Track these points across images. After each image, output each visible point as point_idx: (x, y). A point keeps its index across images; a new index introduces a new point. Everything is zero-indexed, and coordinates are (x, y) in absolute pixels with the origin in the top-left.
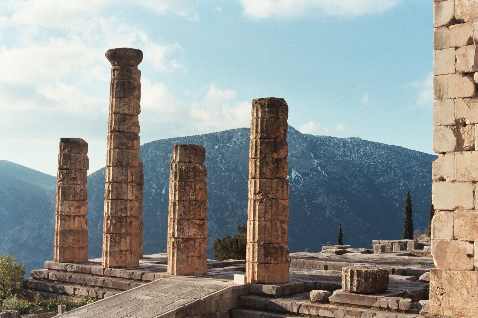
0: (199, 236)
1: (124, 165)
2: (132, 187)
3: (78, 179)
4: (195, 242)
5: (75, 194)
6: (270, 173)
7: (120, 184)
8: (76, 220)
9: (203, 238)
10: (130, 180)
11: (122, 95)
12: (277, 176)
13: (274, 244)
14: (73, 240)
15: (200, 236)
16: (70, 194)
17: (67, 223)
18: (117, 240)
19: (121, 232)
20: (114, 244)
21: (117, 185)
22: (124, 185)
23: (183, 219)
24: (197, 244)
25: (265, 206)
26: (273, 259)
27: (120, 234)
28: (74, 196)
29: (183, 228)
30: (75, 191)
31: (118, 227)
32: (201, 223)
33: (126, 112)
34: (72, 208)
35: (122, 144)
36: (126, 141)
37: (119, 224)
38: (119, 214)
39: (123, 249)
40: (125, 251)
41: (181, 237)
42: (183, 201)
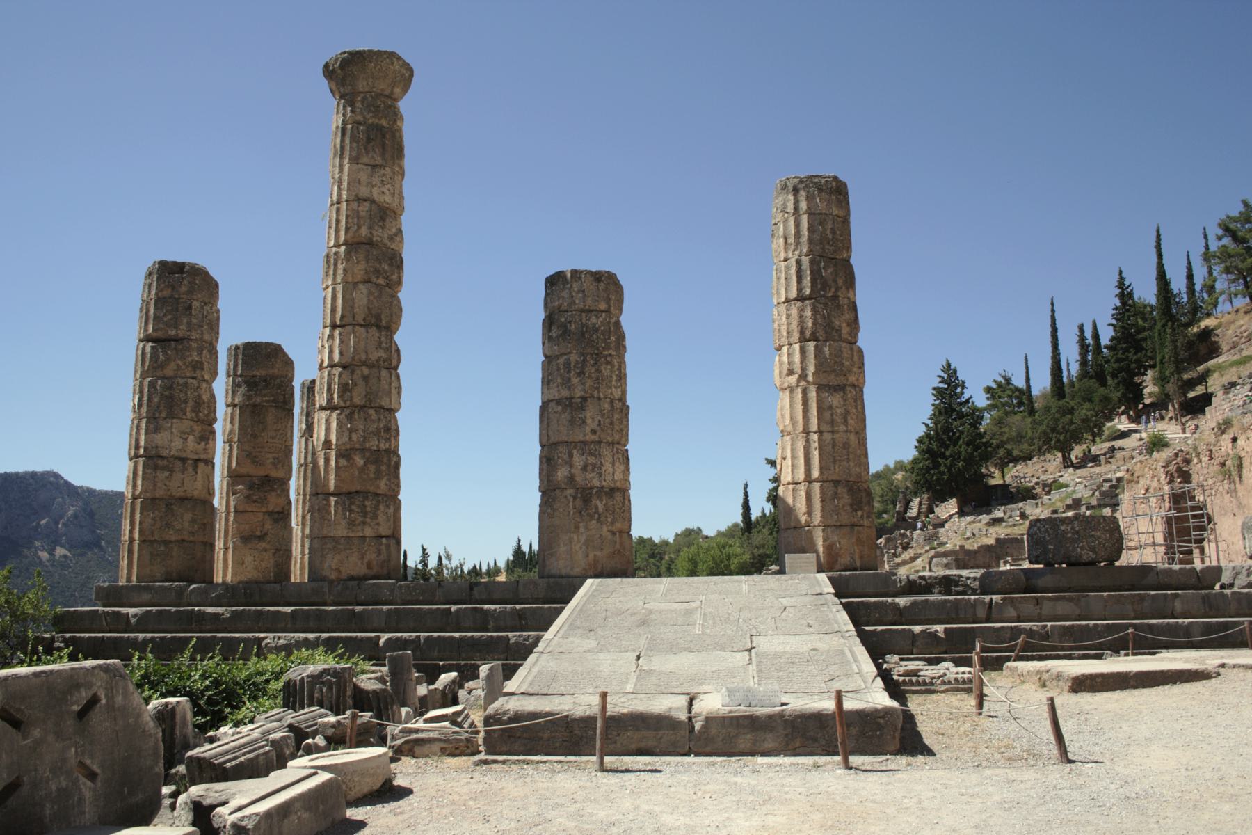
1: (384, 323)
3: (206, 365)
5: (199, 403)
7: (375, 370)
11: (379, 160)
14: (193, 521)
16: (186, 402)
17: (178, 476)
18: (368, 509)
19: (379, 487)
20: (361, 519)
21: (366, 371)
22: (384, 373)
23: (600, 442)
27: (376, 494)
28: (196, 410)
30: (200, 396)
31: (372, 475)
33: (388, 198)
34: (191, 438)
36: (386, 267)
37: (372, 468)
38: (373, 443)
40: (387, 537)
41: (596, 483)
42: (599, 399)
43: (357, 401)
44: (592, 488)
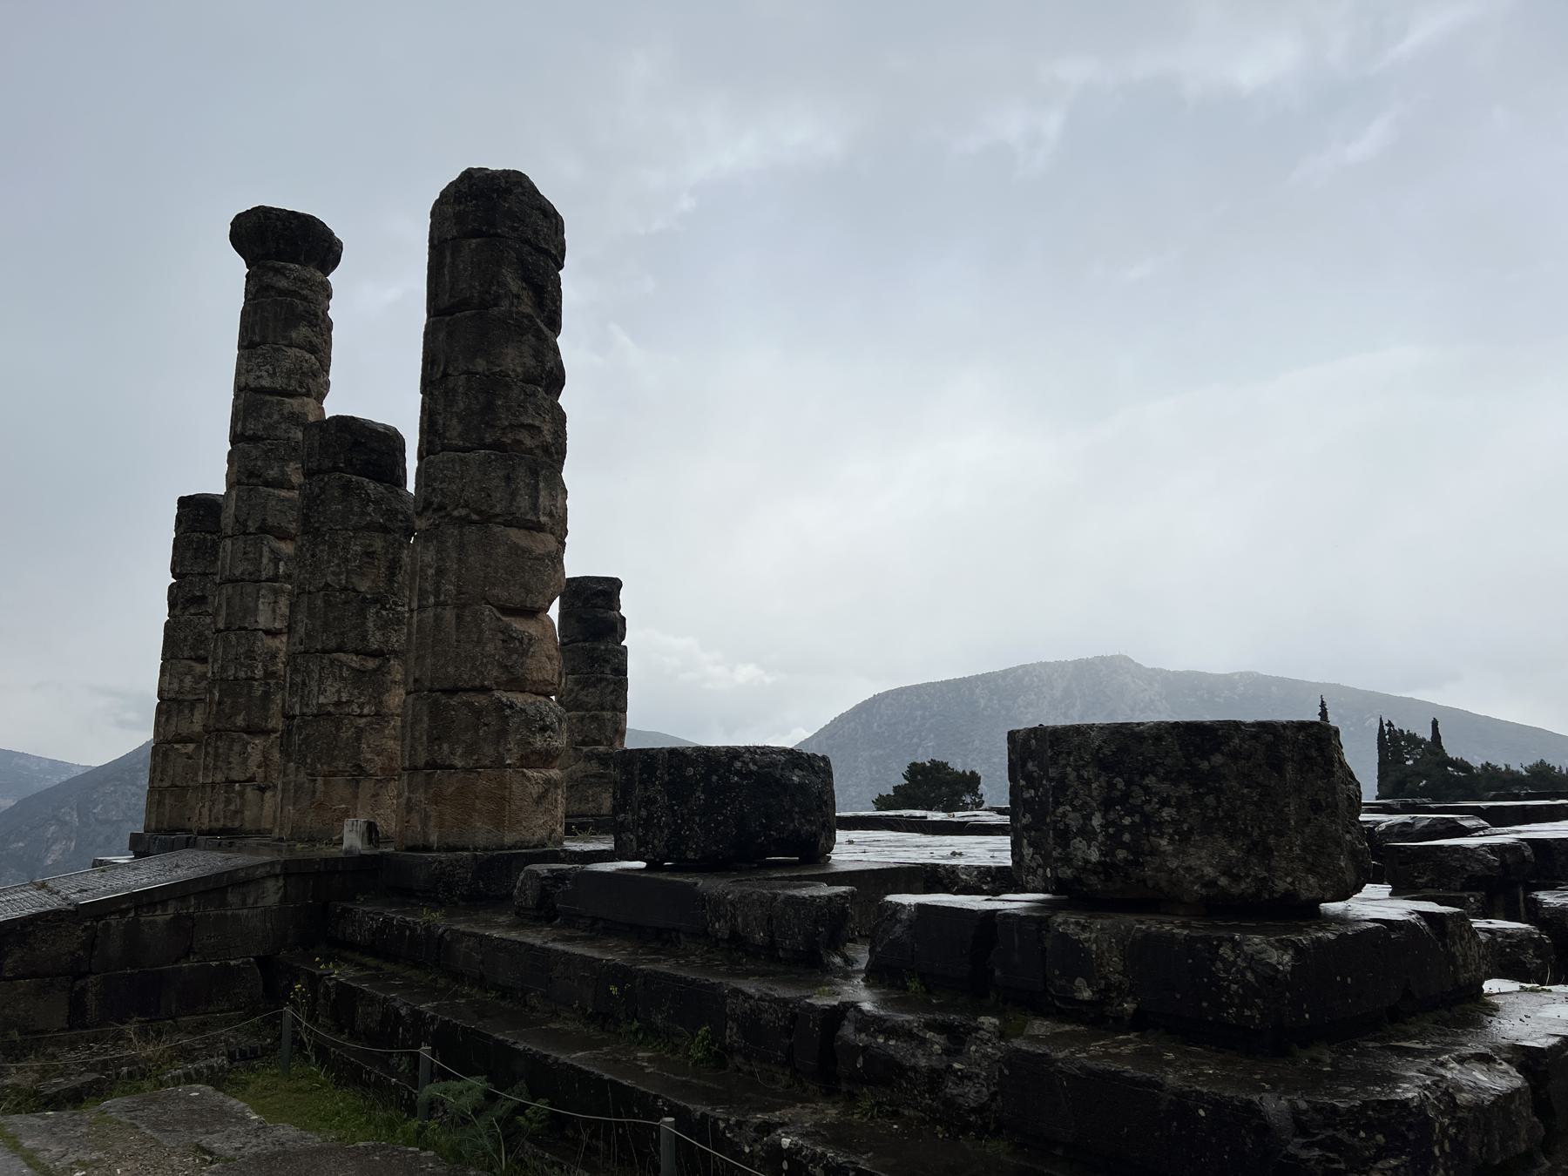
0: (355, 707)
2: (276, 593)
4: (338, 729)
6: (459, 428)
8: (197, 714)
9: (377, 714)
10: (267, 570)
11: (257, 339)
12: (488, 440)
13: (466, 690)
15: (361, 706)
17: (174, 721)
22: (250, 588)
24: (347, 734)
25: (438, 552)
26: (459, 751)
29: (304, 683)
30: (201, 634)
32: (371, 664)
33: (266, 383)
35: (251, 475)
39: (234, 775)
43: (221, 626)
44: (294, 717)
